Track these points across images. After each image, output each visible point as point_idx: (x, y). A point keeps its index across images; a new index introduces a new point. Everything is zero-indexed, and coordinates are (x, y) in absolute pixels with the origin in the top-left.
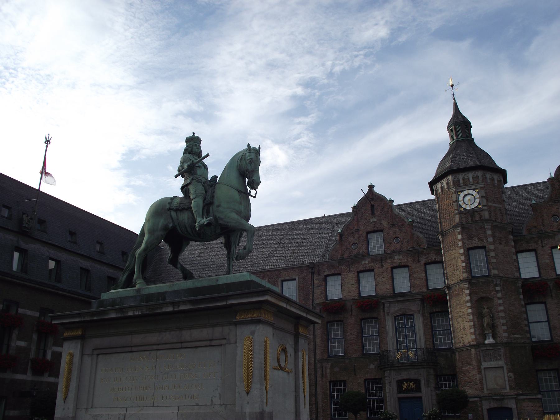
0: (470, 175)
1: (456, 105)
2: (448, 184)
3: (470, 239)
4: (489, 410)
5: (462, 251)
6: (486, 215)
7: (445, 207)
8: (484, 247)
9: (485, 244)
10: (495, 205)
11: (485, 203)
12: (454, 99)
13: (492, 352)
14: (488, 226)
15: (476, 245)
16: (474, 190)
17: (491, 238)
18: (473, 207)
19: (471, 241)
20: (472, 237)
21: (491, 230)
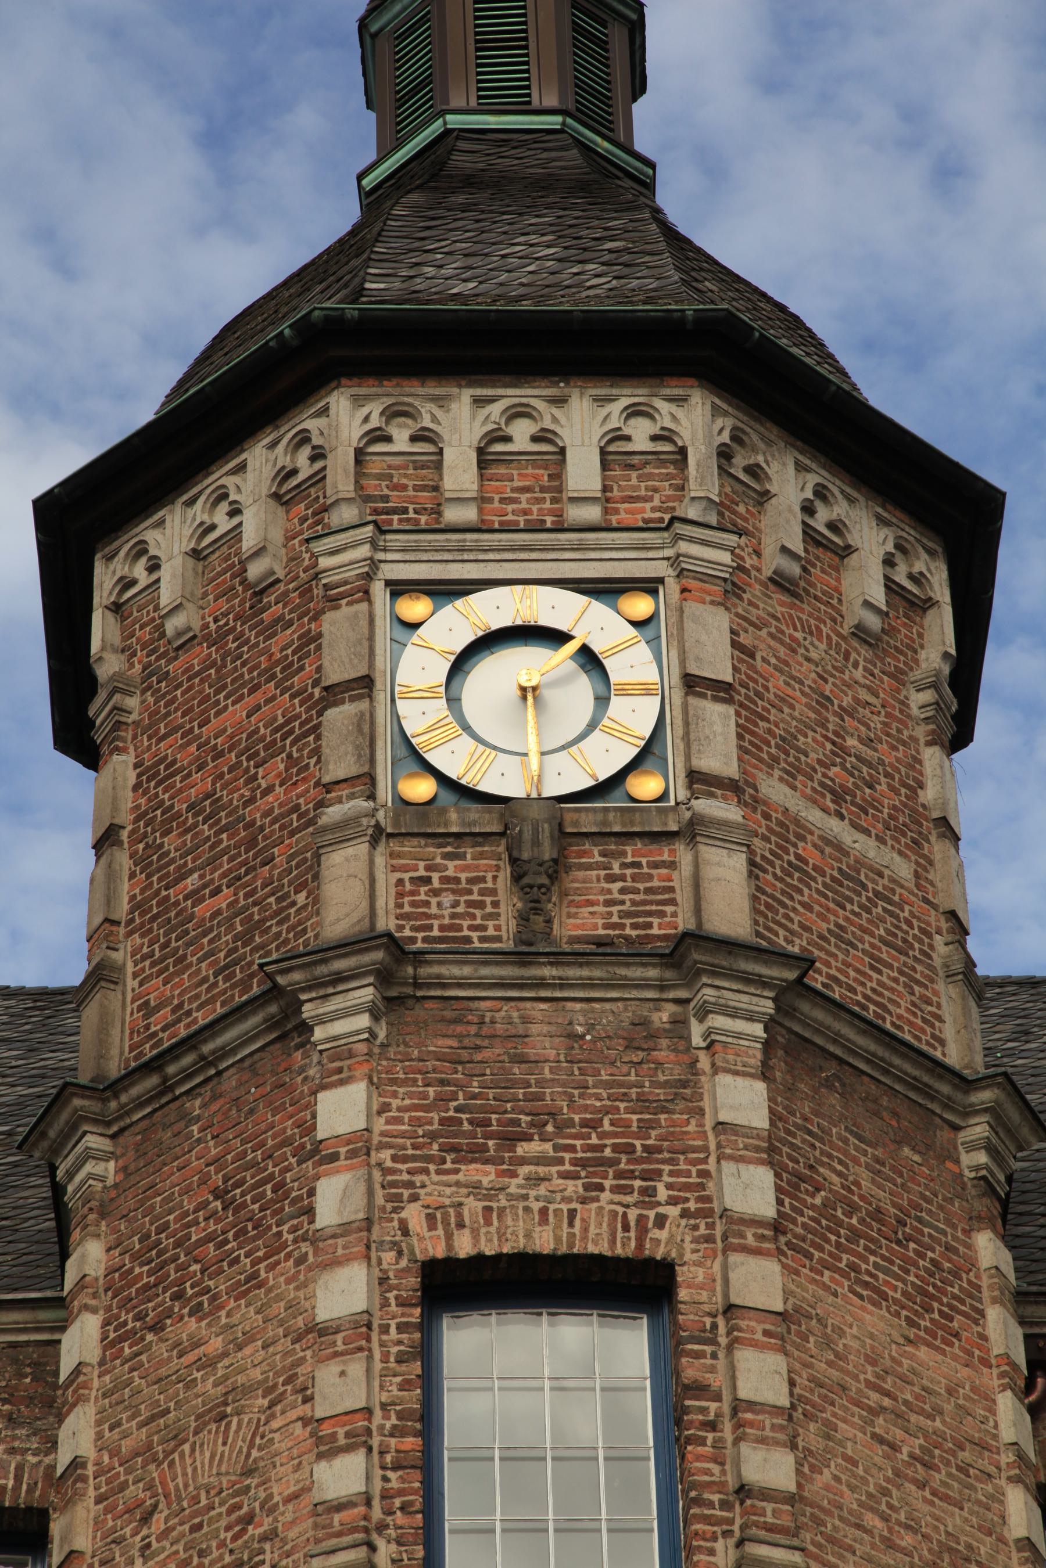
0: (583, 421)
2: (286, 492)
3: (476, 1154)
5: (343, 1292)
6: (724, 892)
7: (201, 783)
8: (631, 1285)
9: (661, 1243)
10: (837, 828)
11: (720, 757)
14: (740, 1019)
15: (544, 1241)
17: (763, 1177)
18: (569, 777)
19: (486, 1175)
20: (511, 1138)
21: (765, 1074)
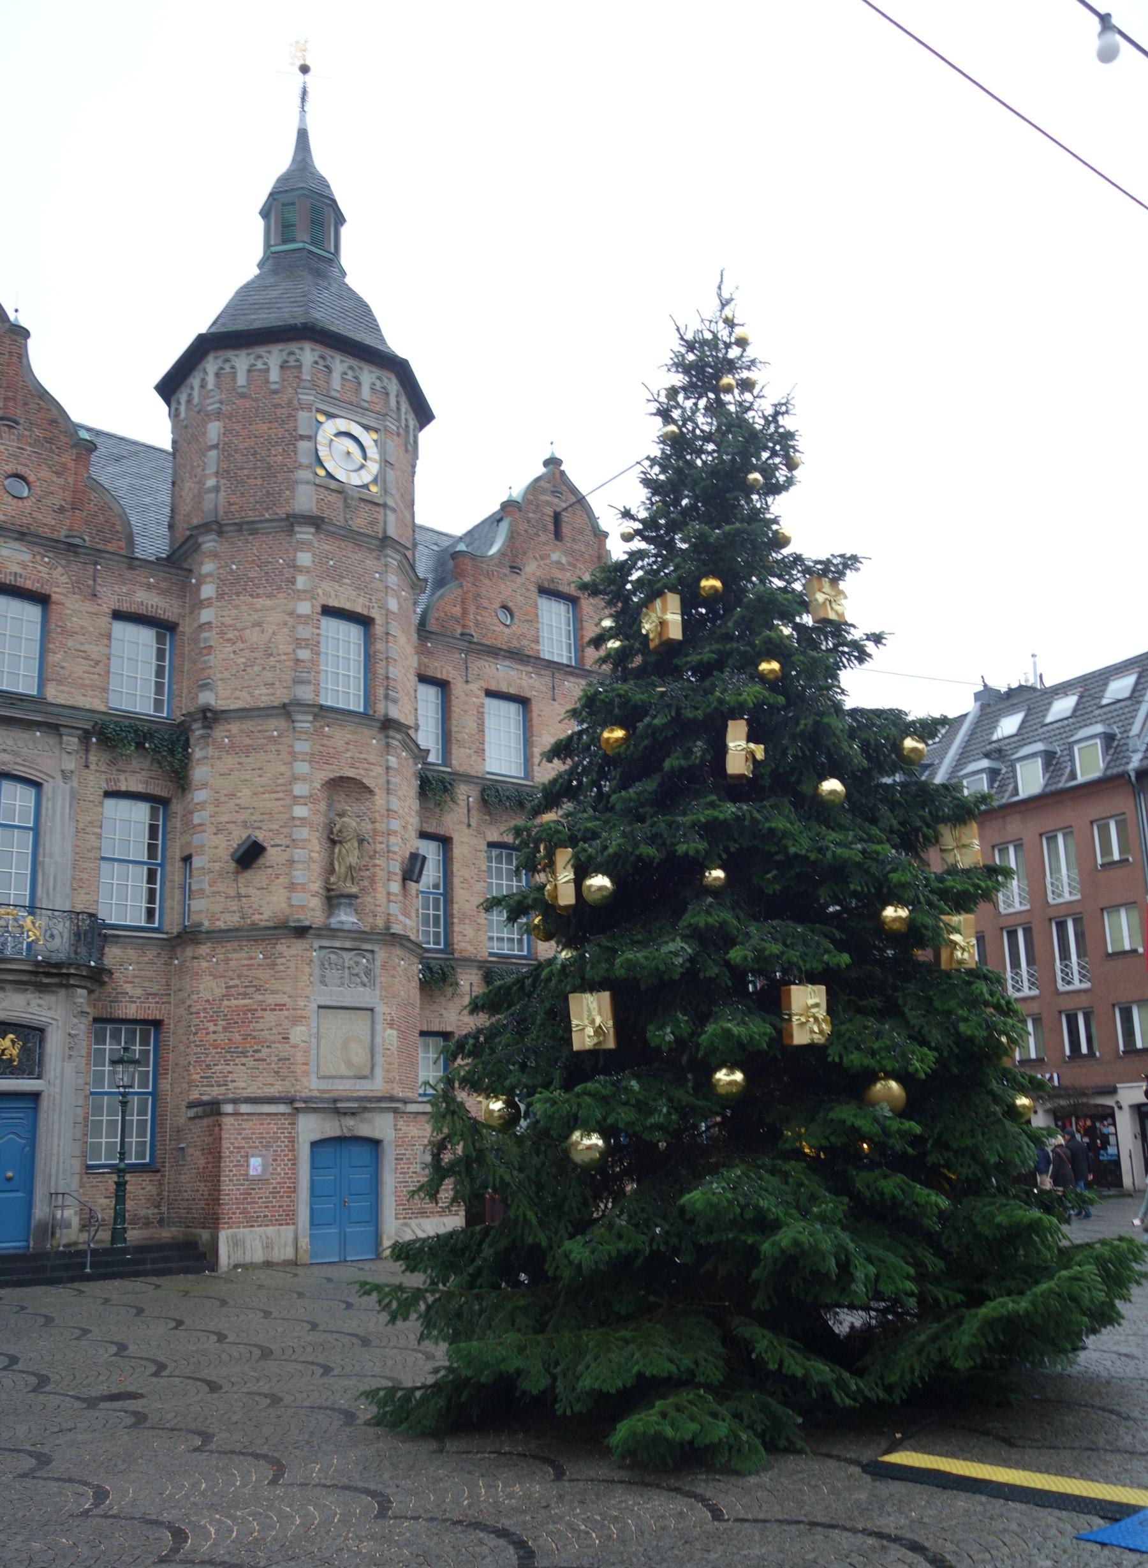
1: (303, 136)
3: (333, 579)
4: (314, 1144)
9: (374, 613)
12: (303, 110)
13: (346, 955)
16: (367, 428)
